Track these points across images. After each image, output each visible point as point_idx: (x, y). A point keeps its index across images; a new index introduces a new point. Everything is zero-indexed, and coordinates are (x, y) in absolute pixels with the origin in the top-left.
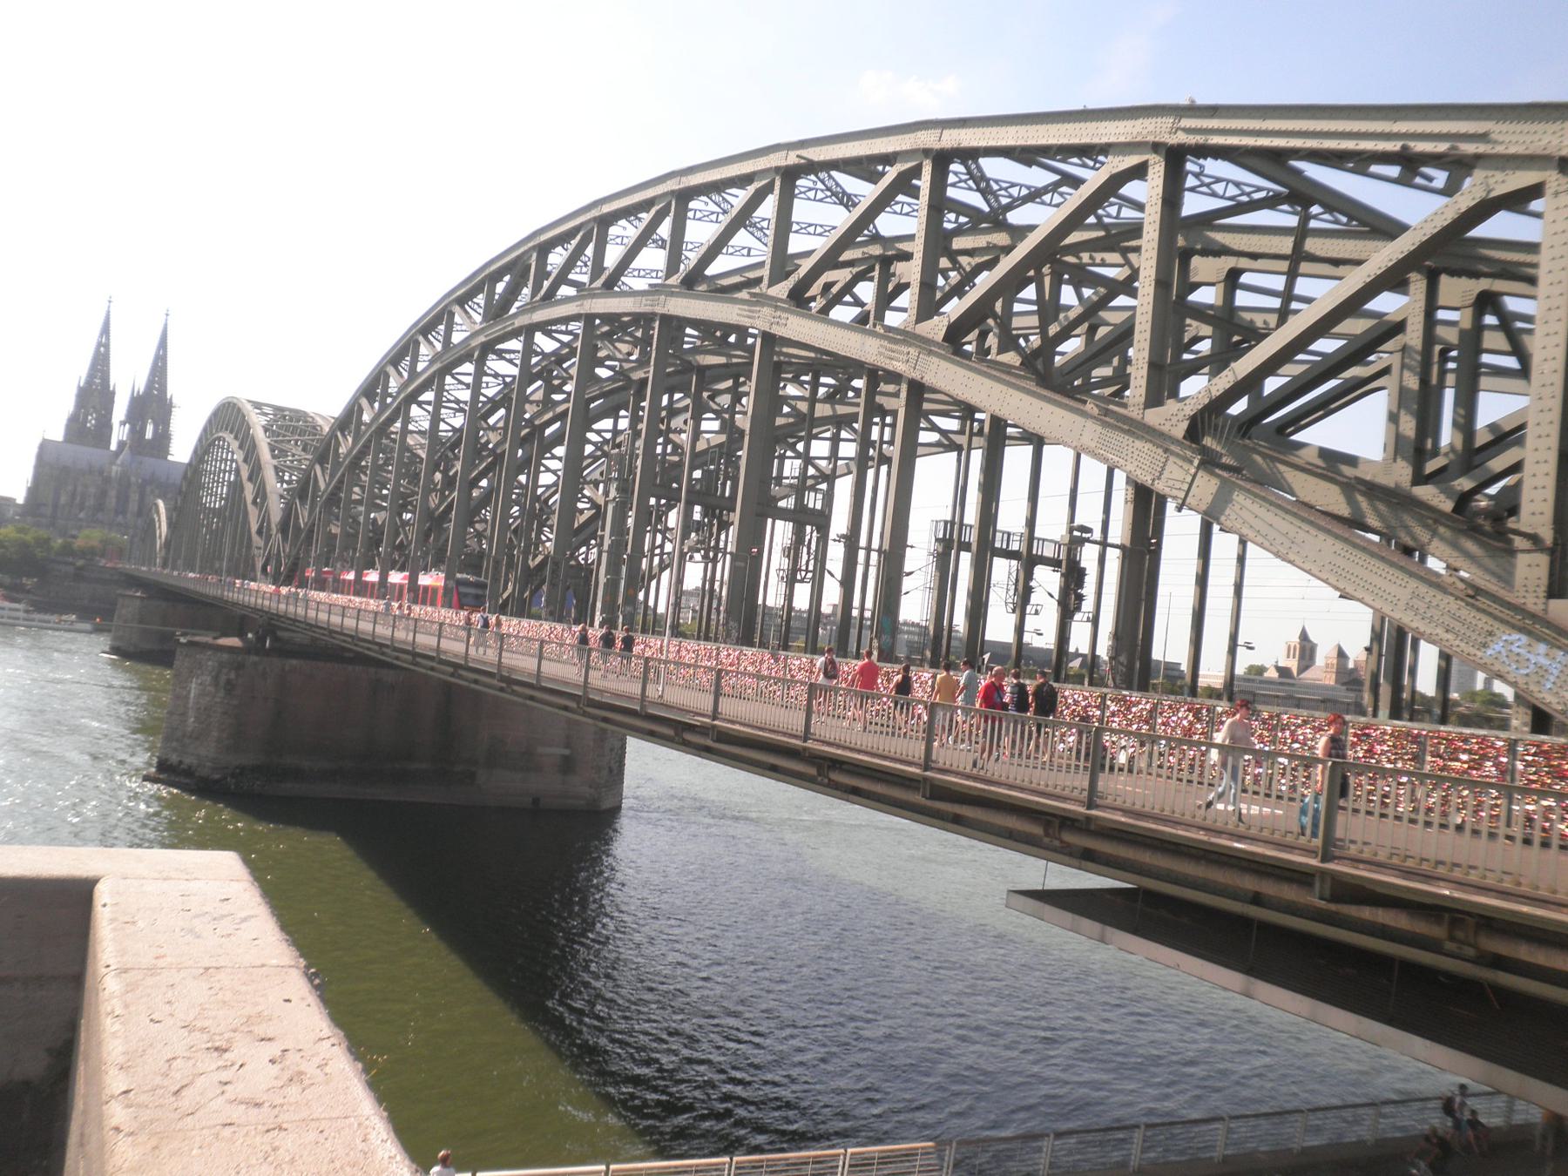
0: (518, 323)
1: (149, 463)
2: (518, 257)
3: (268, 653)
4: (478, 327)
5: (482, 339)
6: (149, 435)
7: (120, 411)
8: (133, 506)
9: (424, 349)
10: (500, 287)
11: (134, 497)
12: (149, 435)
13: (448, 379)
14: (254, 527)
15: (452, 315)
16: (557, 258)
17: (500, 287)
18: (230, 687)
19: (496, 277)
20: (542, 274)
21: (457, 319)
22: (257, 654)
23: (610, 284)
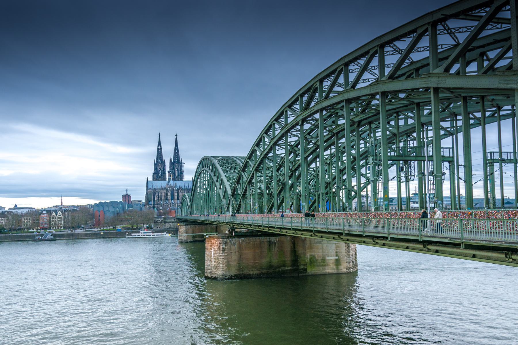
0: (316, 109)
1: (179, 183)
2: (312, 86)
3: (234, 237)
4: (299, 114)
5: (301, 117)
6: (177, 174)
7: (167, 169)
8: (176, 197)
9: (277, 126)
10: (305, 99)
11: (176, 194)
12: (177, 174)
13: (289, 134)
14: (222, 196)
15: (286, 111)
16: (327, 83)
17: (305, 99)
18: (224, 250)
19: (302, 95)
20: (322, 91)
21: (289, 113)
22: (231, 238)
23: (354, 86)
